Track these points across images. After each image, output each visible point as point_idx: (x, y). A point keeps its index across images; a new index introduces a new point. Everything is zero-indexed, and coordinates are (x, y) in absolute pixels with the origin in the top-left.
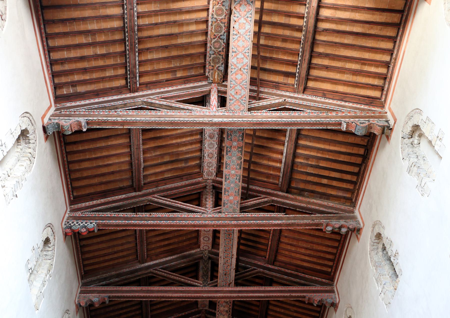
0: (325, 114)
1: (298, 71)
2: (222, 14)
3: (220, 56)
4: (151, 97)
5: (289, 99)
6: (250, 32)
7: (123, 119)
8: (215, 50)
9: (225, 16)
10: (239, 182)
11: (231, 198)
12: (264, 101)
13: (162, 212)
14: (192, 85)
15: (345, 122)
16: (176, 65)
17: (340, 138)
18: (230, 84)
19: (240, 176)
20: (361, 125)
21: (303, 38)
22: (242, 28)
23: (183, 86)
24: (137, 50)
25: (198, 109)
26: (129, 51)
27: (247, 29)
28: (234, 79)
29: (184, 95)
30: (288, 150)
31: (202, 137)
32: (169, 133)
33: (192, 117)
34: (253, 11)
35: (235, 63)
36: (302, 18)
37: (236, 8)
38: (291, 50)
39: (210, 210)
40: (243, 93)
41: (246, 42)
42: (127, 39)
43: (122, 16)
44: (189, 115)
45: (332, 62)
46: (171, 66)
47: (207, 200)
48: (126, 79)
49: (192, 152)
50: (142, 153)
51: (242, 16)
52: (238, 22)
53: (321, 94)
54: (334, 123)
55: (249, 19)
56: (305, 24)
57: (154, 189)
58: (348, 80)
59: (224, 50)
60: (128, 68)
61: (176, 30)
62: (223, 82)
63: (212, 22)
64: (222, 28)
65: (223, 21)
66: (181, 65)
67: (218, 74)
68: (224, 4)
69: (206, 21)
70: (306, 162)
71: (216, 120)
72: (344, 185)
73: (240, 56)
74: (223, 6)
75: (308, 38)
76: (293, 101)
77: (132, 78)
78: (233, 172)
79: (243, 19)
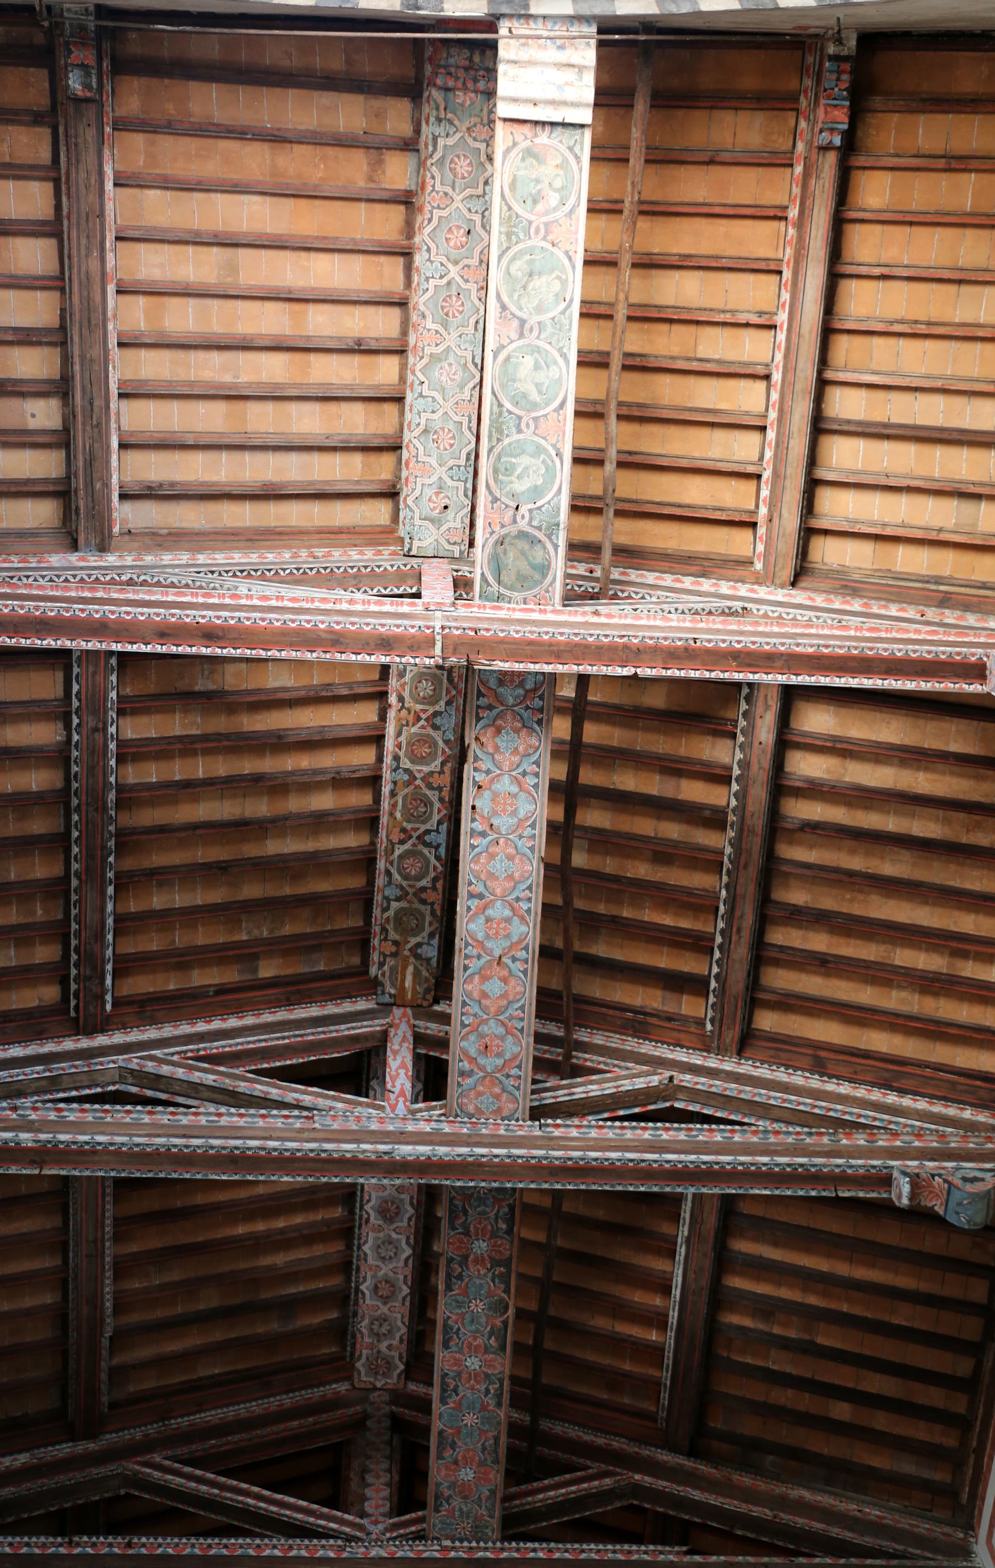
0: (825, 1140)
1: (715, 970)
2: (431, 756)
3: (422, 908)
4: (157, 1053)
5: (688, 1077)
6: (533, 826)
7: (43, 1137)
8: (405, 883)
9: (443, 764)
10: (499, 1404)
11: (467, 1474)
12: (592, 1083)
13: (181, 1536)
14: (314, 1011)
15: (905, 1174)
16: (256, 933)
17: (890, 1235)
18: (463, 1014)
19: (501, 1381)
20: (969, 1188)
21: (728, 850)
22: (504, 811)
23: (282, 1015)
24: (110, 875)
25: (340, 1105)
26: (79, 878)
27: (522, 814)
28: (476, 995)
29: (286, 1047)
30: (691, 1276)
31: (352, 1212)
32: (222, 1197)
33: (313, 1135)
34: (544, 752)
35: (480, 936)
36: (723, 778)
37: (484, 740)
38: (689, 892)
39: (381, 1527)
40: (510, 1047)
41: (521, 860)
42: (75, 834)
43: (60, 752)
44: (301, 1130)
45: (842, 941)
46: (236, 938)
47: (370, 1479)
48: (64, 982)
49: (312, 1274)
50: (109, 1274)
52: (490, 789)
53: (806, 1062)
54: (864, 1177)
55: (531, 780)
56: (734, 802)
57: (152, 1430)
58: (904, 1009)
59: (439, 885)
60: (74, 943)
61: (260, 808)
62: (436, 1001)
63: (395, 783)
64: (432, 805)
65: (436, 781)
66: (277, 934)
67: (417, 974)
68: (438, 721)
69: (373, 781)
70: (760, 1326)
71: (406, 1150)
72: (921, 1432)
73: (499, 911)
74: (436, 727)
75: (749, 853)
76: (702, 1083)
77: (88, 979)
78: (473, 1363)
79: (506, 779)
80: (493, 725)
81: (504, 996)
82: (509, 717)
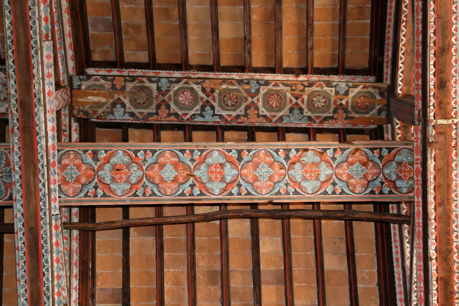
6: (296, 193)
18: (145, 151)
22: (306, 172)
27: (304, 184)
28: (162, 160)
35: (209, 160)
41: (270, 186)
51: (337, 171)
52: (321, 160)
55: (330, 189)
79: (330, 171)
80: (368, 160)
81: (163, 180)
82: (375, 171)
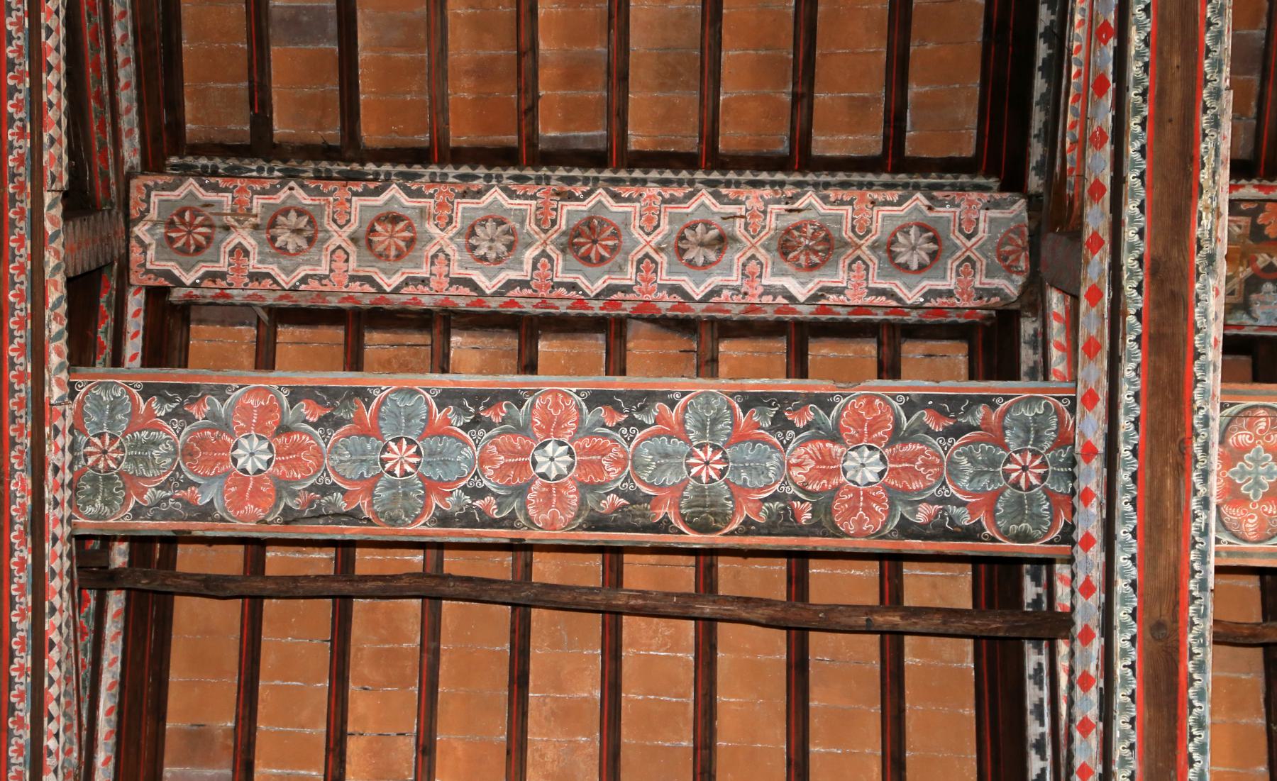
19: (509, 522)
